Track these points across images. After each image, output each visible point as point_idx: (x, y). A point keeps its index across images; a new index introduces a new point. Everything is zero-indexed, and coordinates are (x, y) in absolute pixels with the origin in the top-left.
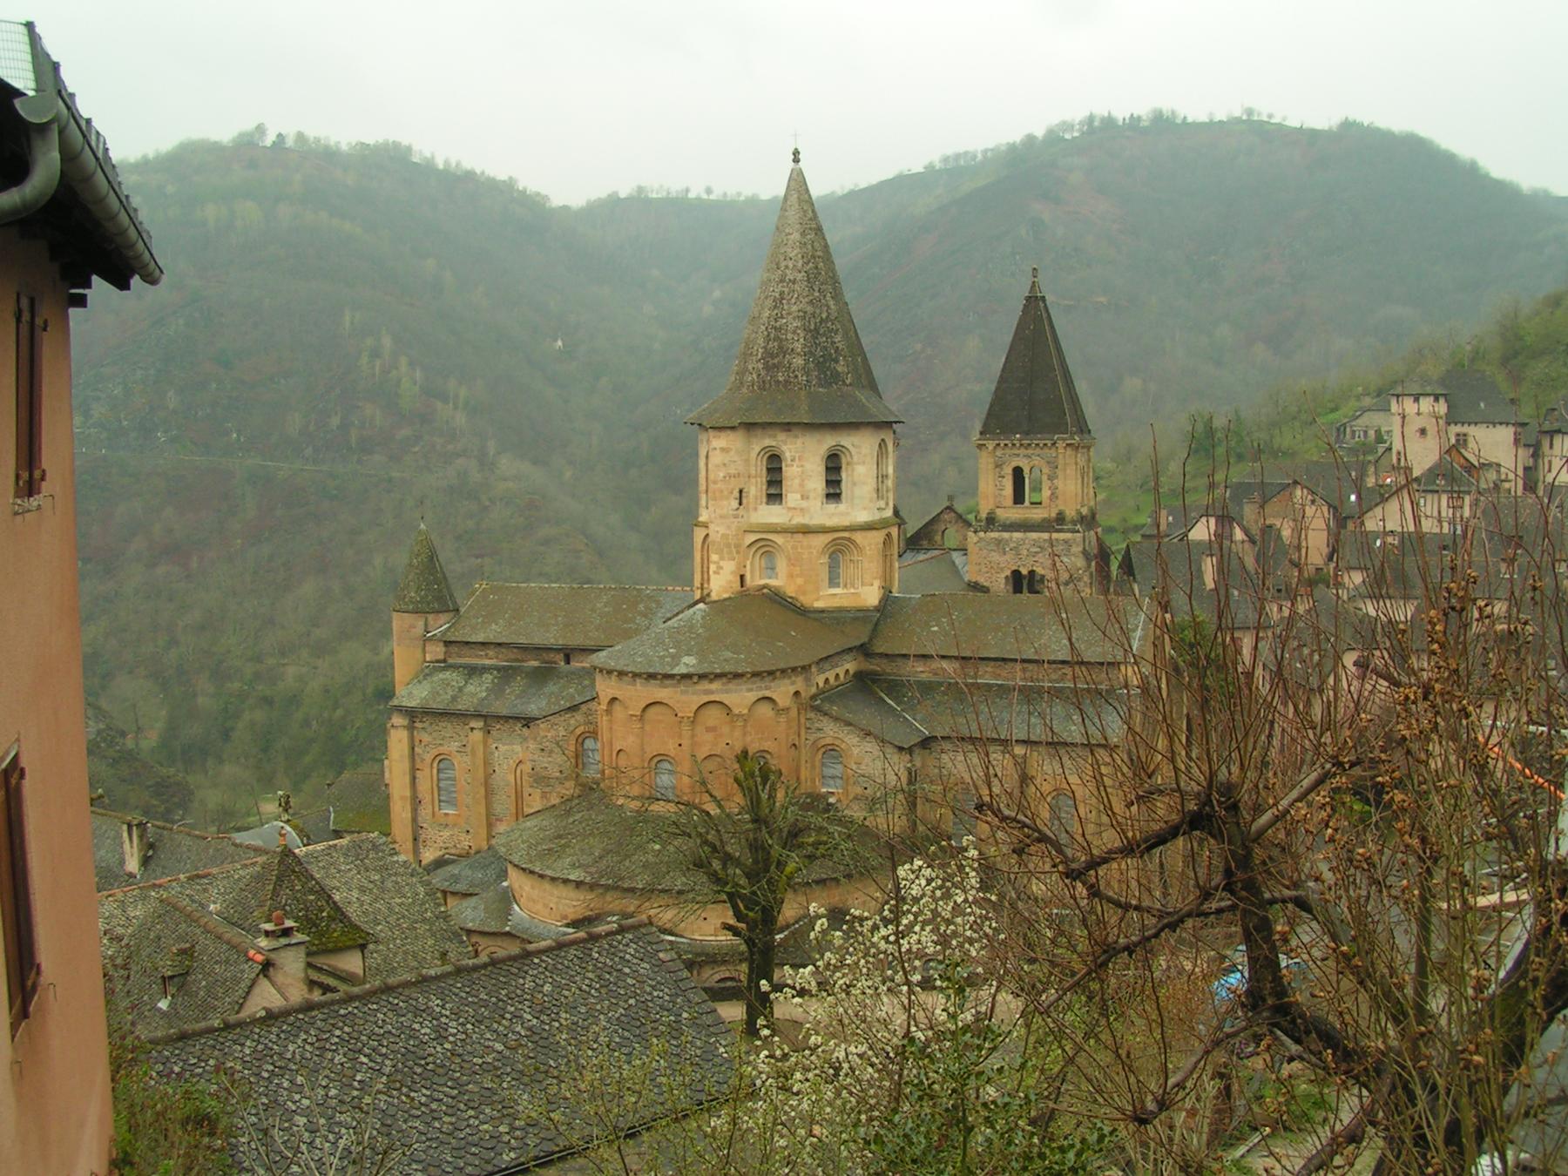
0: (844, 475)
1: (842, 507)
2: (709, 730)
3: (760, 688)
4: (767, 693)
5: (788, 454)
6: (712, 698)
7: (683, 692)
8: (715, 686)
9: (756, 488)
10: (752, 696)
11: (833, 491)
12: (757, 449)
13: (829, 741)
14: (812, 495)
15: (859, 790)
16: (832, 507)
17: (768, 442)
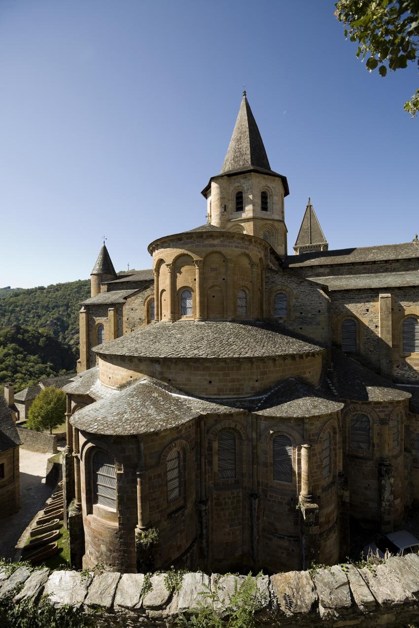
0: (268, 201)
1: (268, 213)
2: (213, 270)
3: (243, 248)
4: (247, 251)
5: (245, 188)
6: (215, 249)
7: (197, 246)
8: (216, 242)
9: (232, 205)
10: (238, 251)
11: (264, 208)
12: (232, 188)
13: (279, 287)
14: (256, 205)
15: (298, 314)
16: (264, 212)
17: (237, 184)
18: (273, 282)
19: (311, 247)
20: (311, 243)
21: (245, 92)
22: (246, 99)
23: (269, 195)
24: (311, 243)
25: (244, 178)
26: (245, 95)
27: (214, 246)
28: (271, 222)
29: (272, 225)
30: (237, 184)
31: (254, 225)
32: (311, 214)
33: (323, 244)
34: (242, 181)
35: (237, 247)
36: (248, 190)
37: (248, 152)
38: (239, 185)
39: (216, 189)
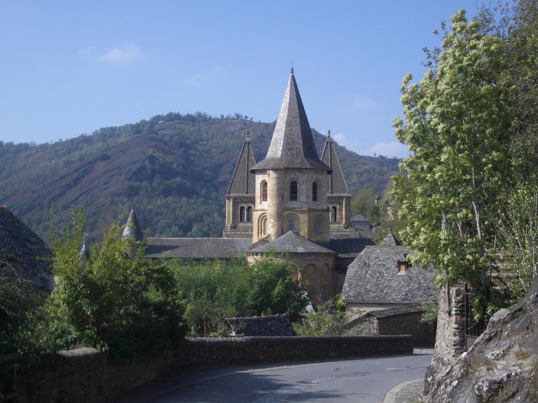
1: (318, 203)
8: (312, 258)
9: (287, 194)
12: (288, 179)
17: (292, 176)
18: (338, 279)
19: (332, 198)
20: (332, 193)
21: (293, 69)
22: (293, 78)
23: (318, 185)
24: (332, 193)
25: (300, 172)
26: (292, 72)
27: (310, 260)
28: (320, 213)
29: (321, 215)
30: (292, 176)
31: (309, 217)
32: (332, 153)
33: (346, 196)
34: (298, 174)
35: (323, 260)
36: (303, 183)
37: (301, 141)
38: (295, 177)
39: (274, 179)
